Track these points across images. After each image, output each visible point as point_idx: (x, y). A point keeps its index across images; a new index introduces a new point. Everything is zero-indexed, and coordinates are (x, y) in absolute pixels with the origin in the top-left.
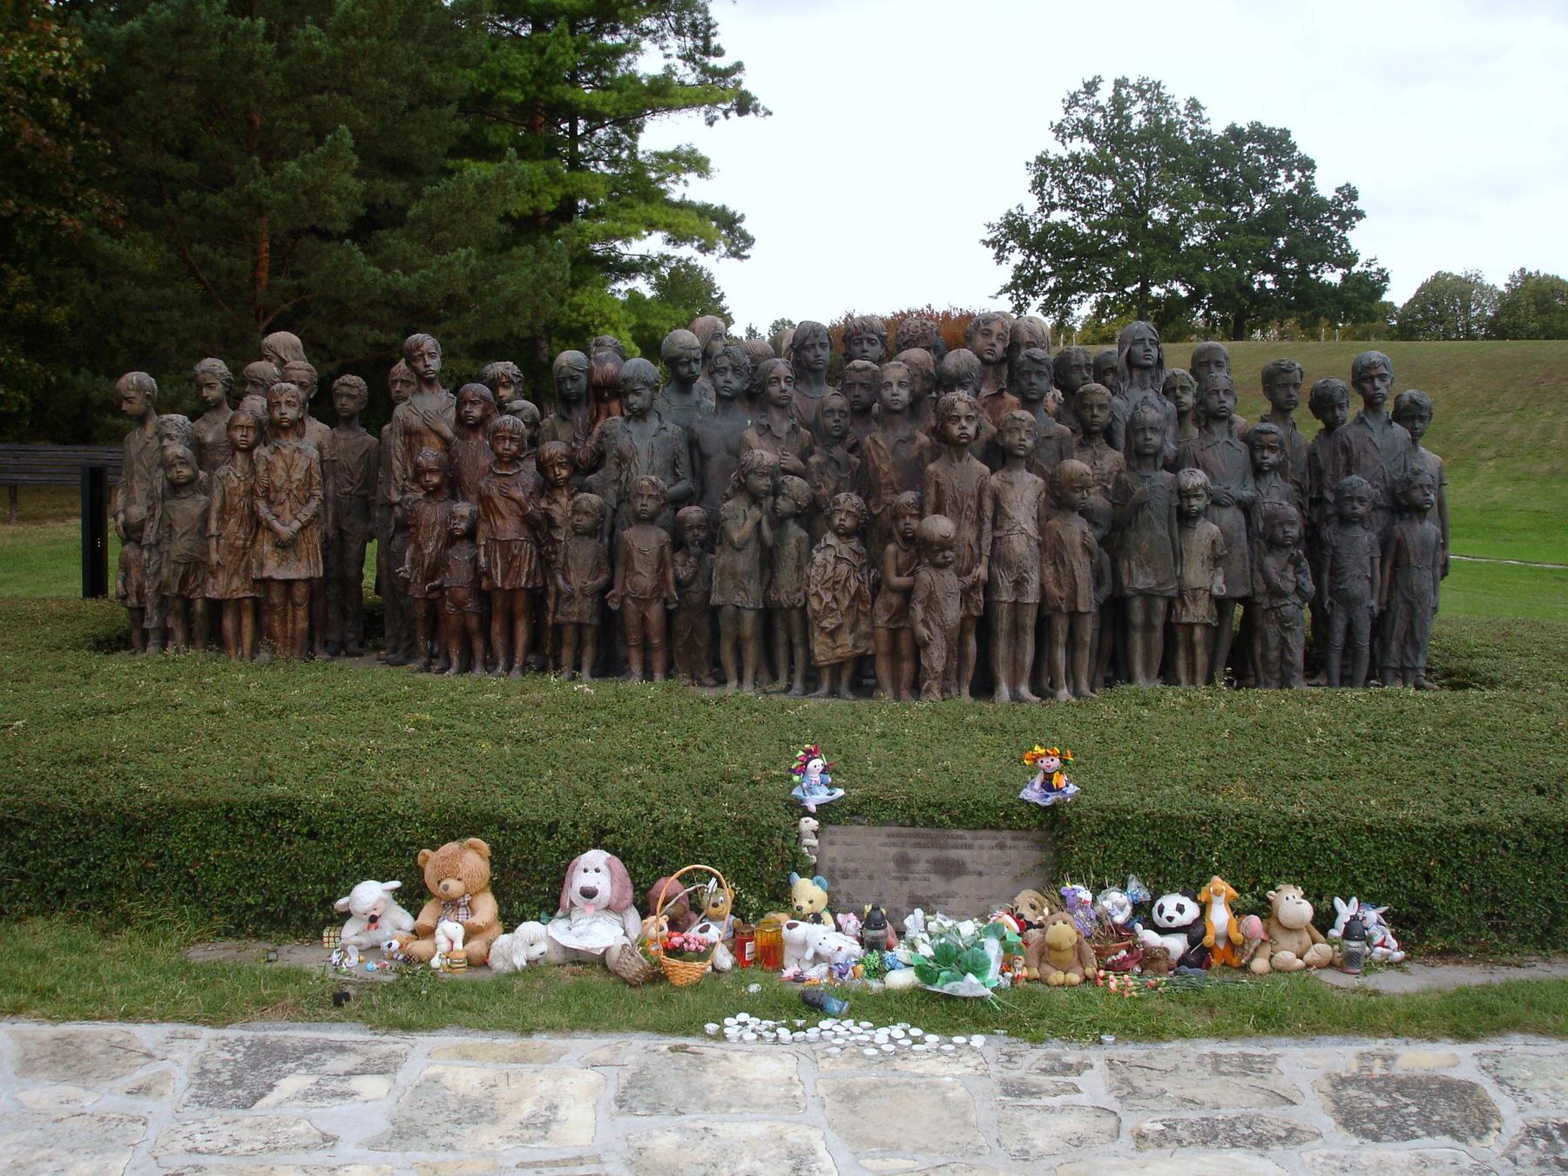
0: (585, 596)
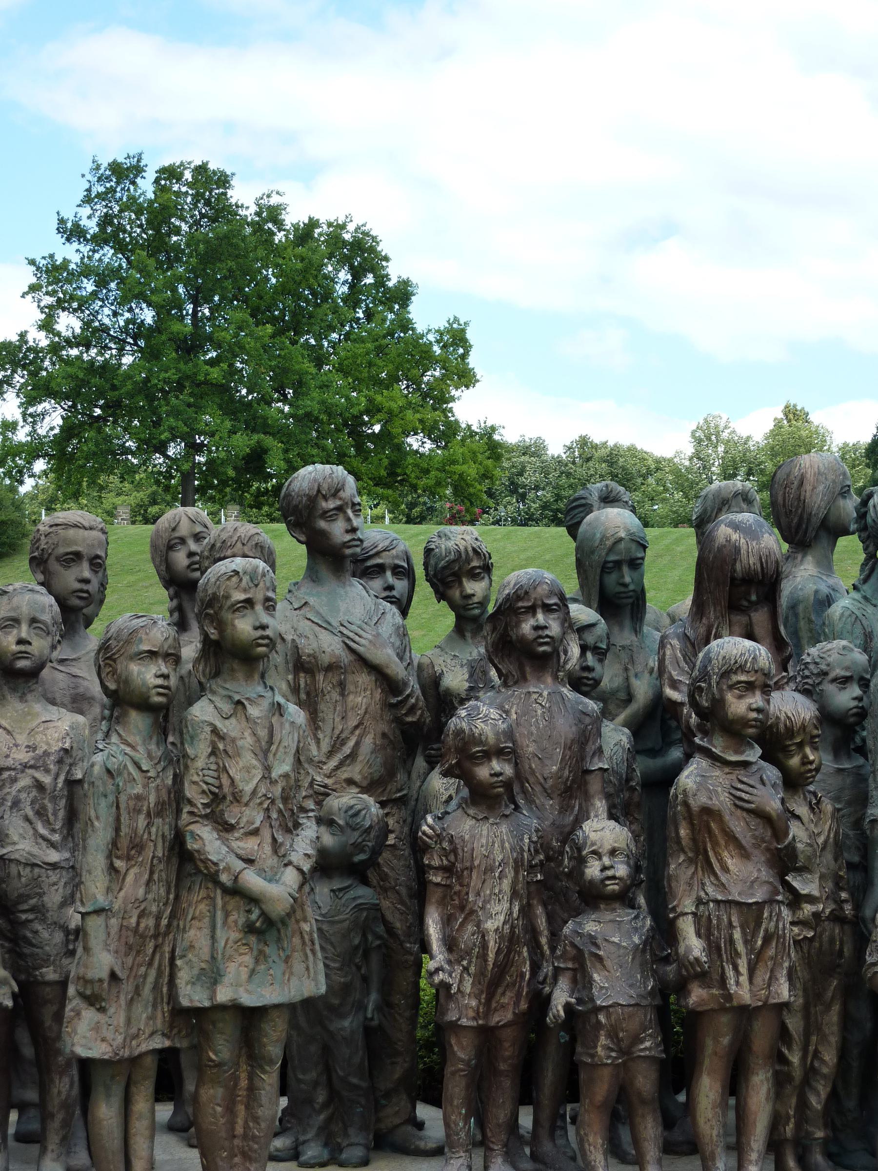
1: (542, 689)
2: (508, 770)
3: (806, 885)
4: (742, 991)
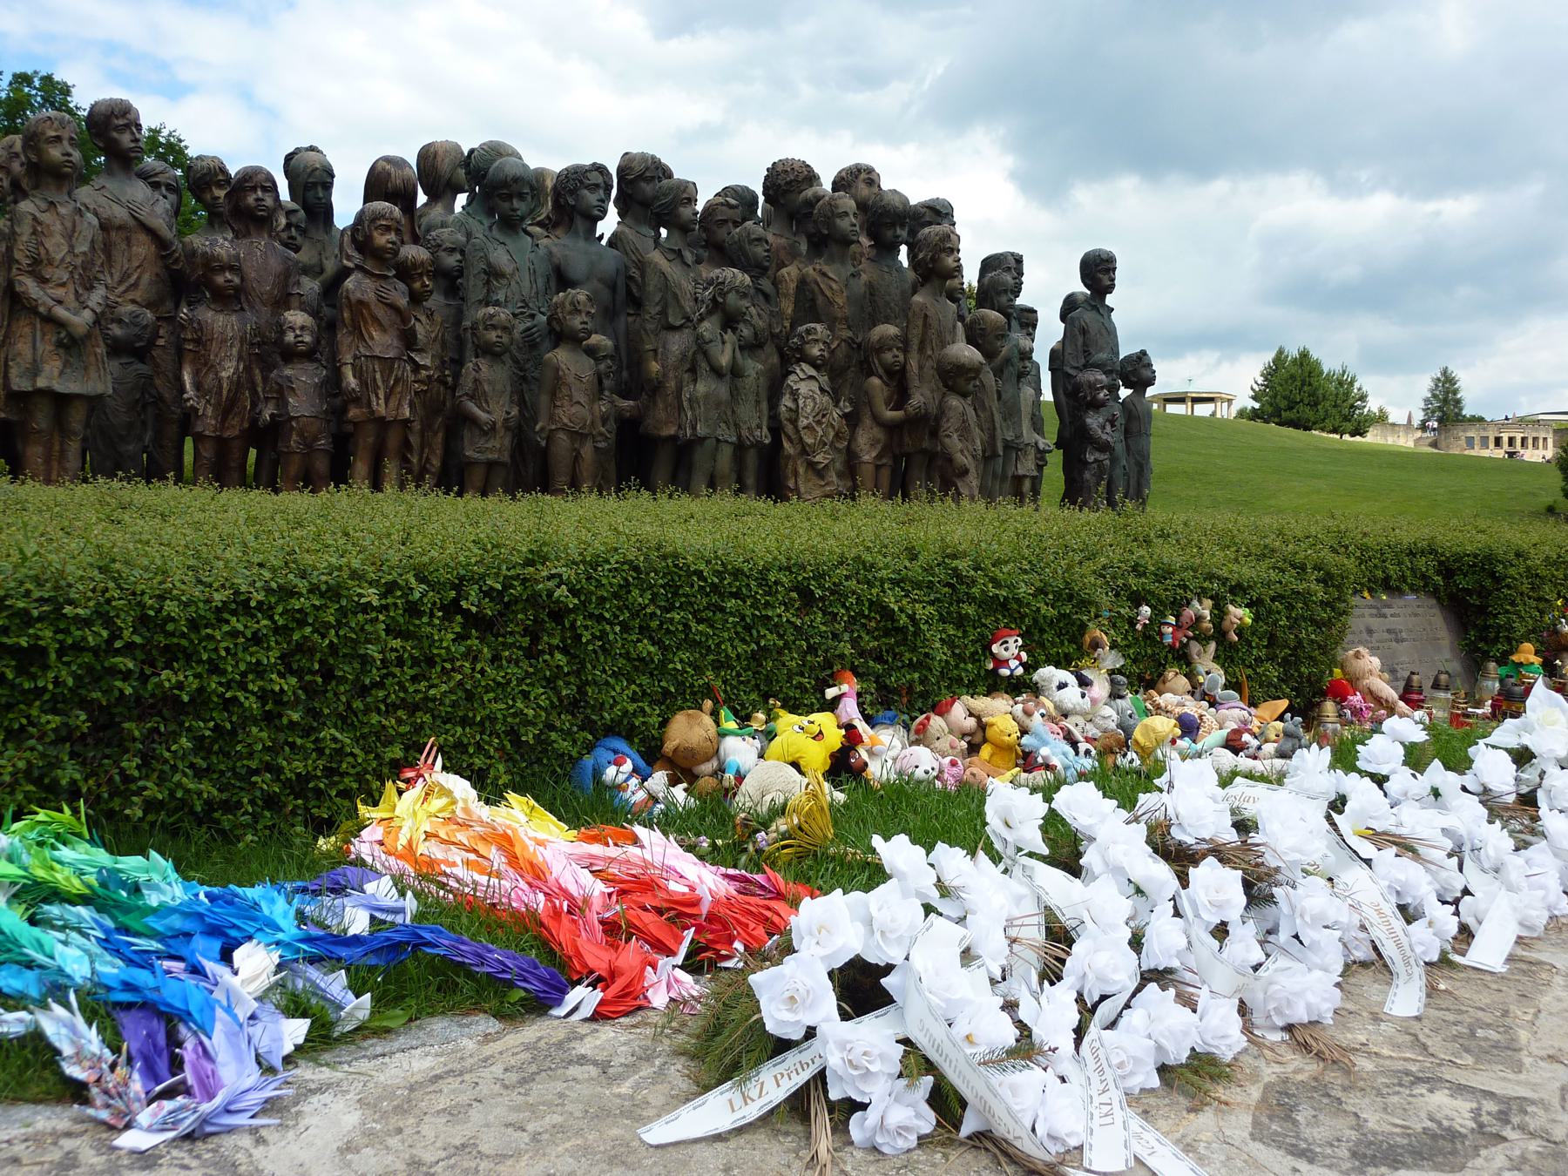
0: (507, 429)
1: (261, 243)
2: (237, 280)
3: (424, 360)
4: (380, 408)
